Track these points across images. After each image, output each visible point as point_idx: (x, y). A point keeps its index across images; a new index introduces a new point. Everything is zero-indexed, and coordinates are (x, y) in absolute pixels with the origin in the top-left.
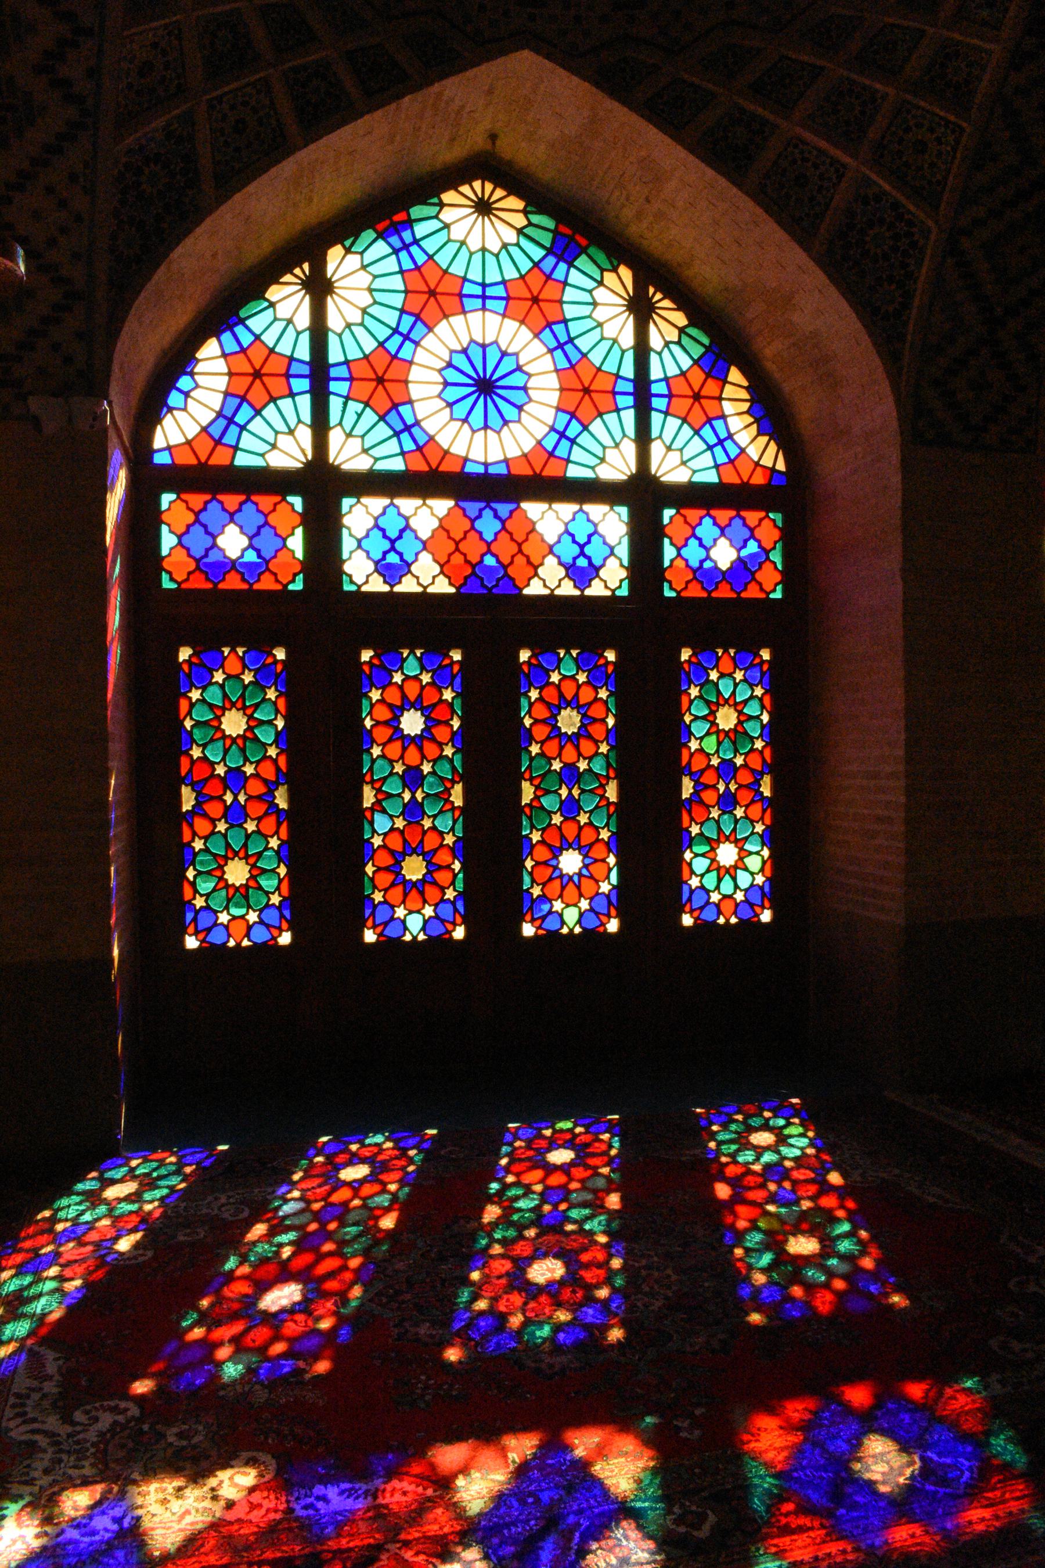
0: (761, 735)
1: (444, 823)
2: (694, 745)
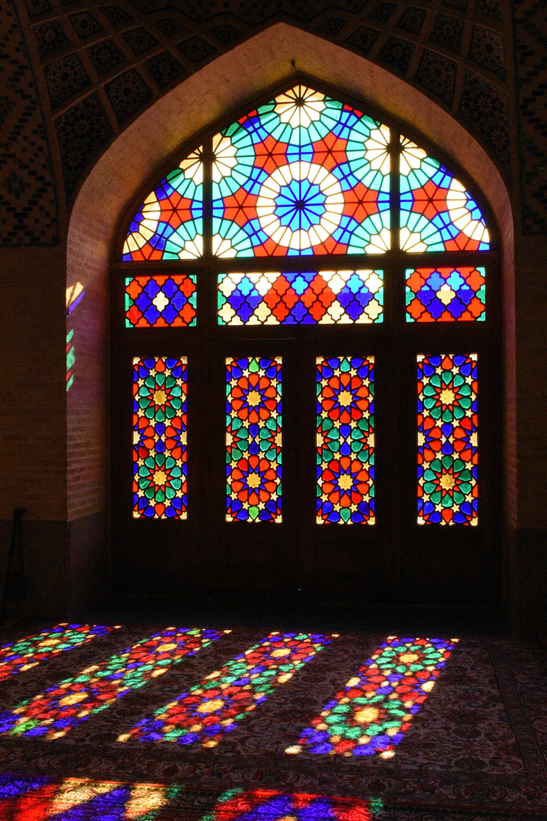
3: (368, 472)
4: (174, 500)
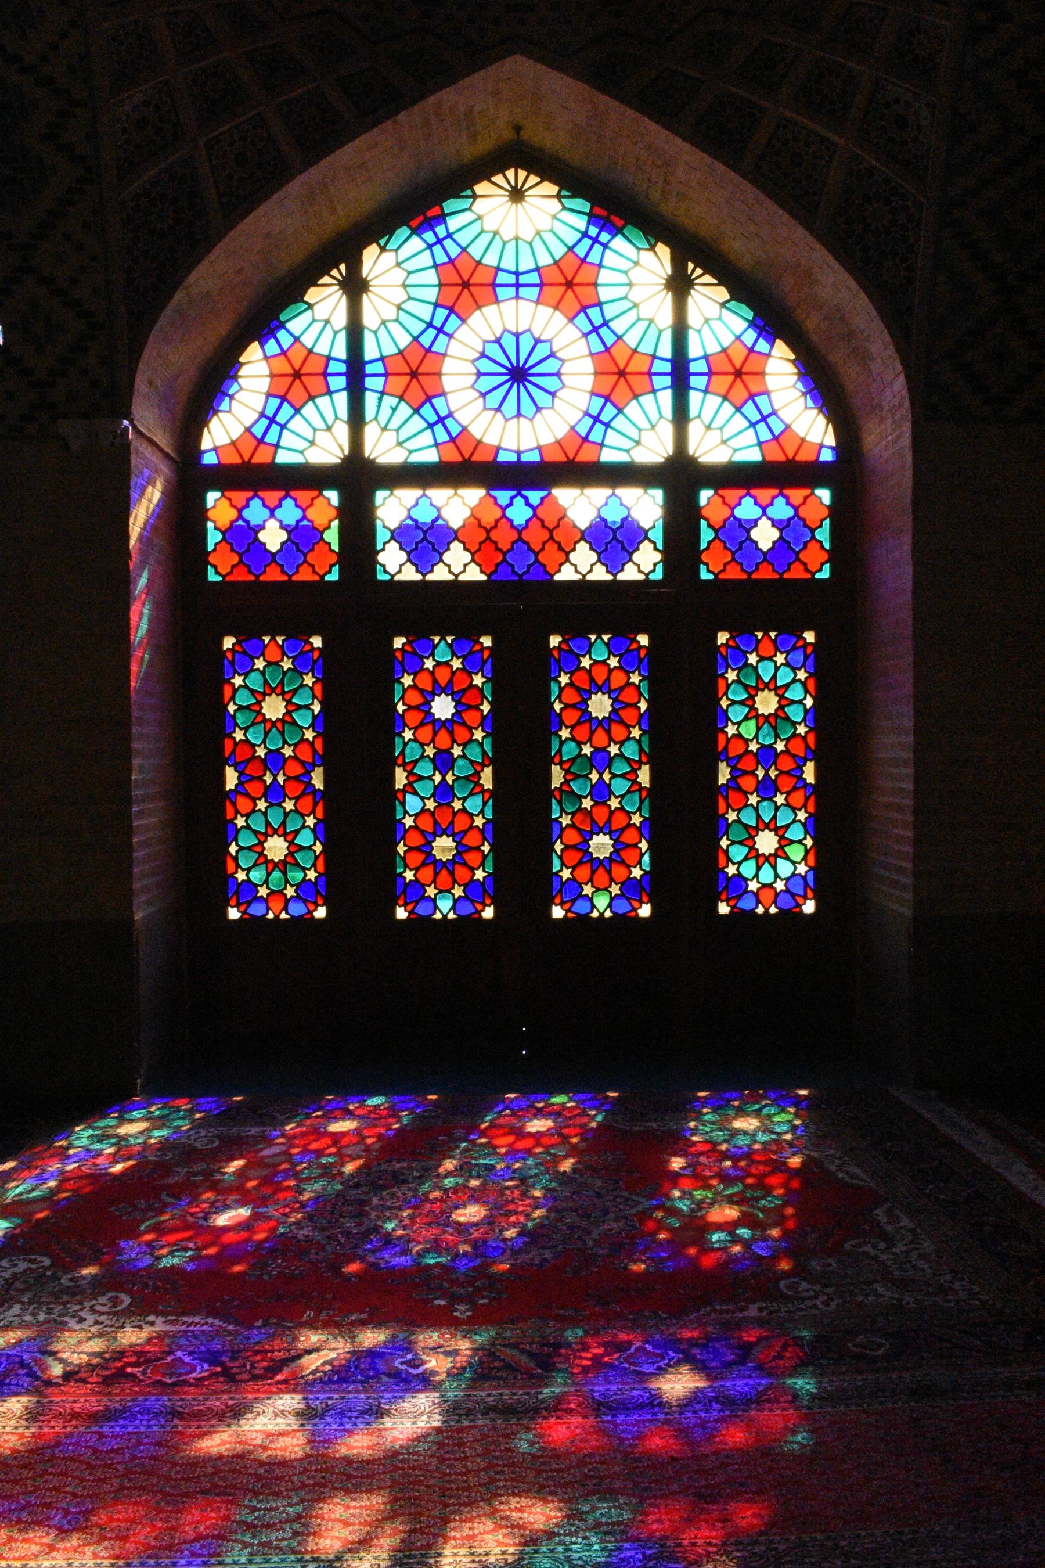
0: (804, 720)
1: (474, 804)
2: (731, 730)
3: (639, 829)
4: (302, 886)
